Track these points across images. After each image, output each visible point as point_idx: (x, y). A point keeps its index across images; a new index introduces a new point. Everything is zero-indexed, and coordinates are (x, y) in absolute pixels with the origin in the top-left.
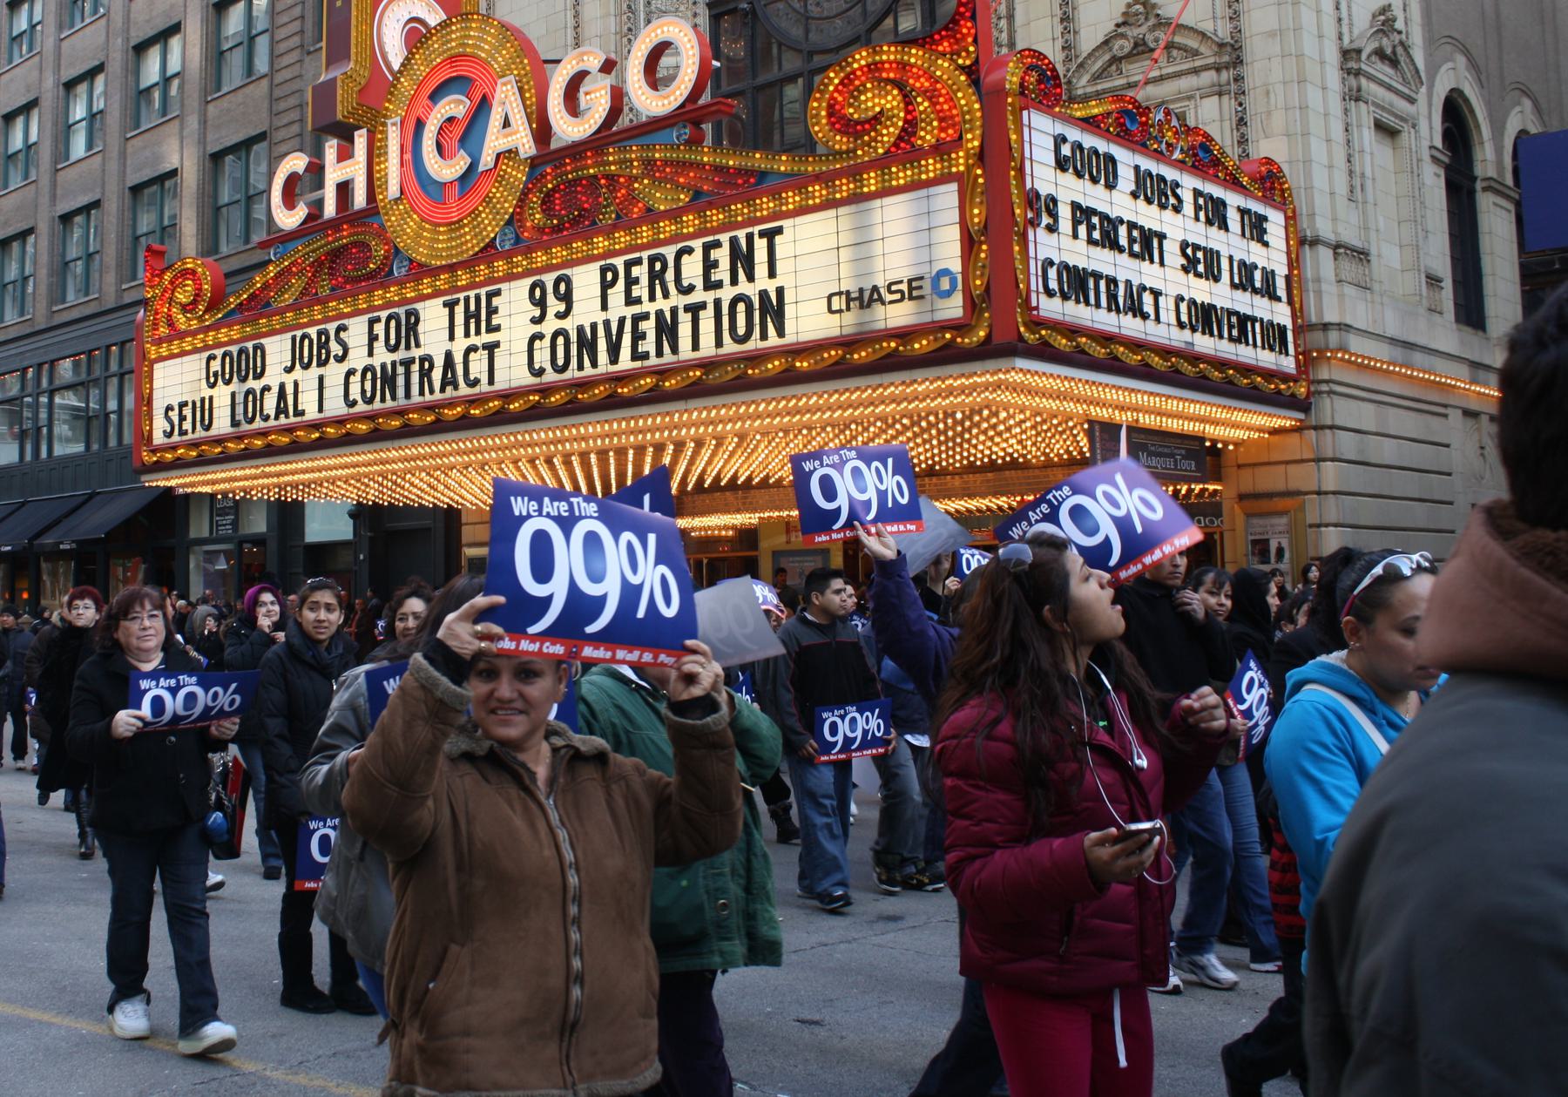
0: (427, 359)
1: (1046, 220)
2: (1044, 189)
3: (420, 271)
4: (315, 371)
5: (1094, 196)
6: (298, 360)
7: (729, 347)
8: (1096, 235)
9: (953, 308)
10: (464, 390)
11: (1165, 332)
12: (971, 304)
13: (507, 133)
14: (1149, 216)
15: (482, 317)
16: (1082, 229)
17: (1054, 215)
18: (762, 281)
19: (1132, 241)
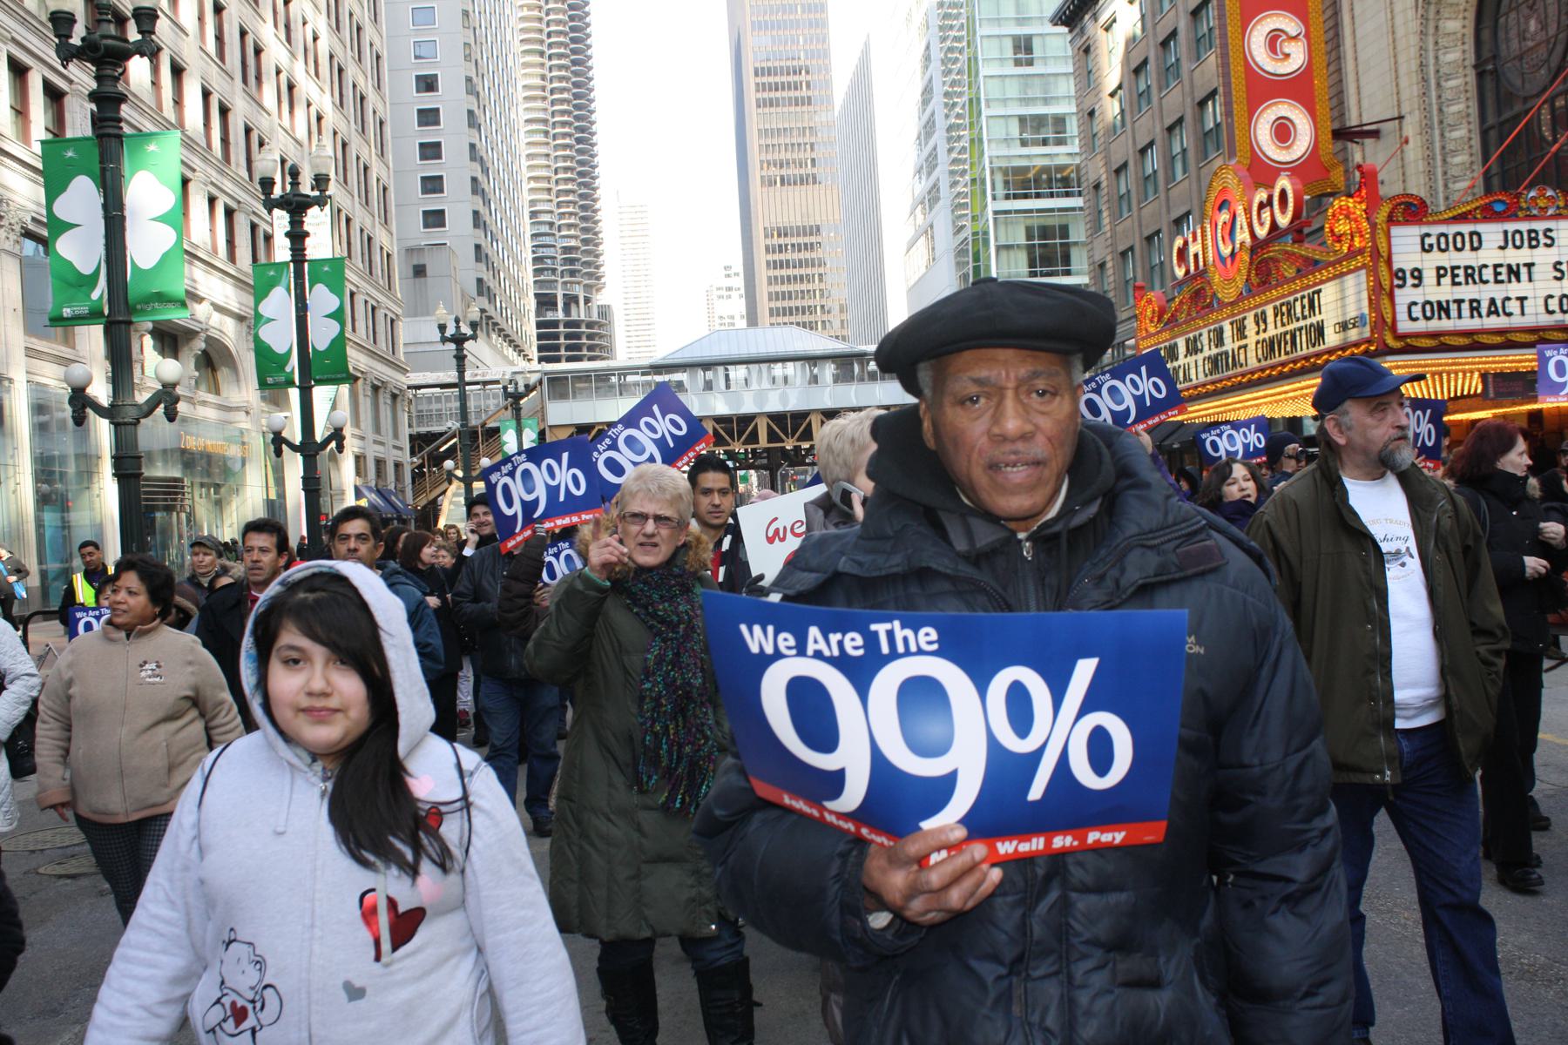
0: (1226, 353)
1: (1410, 281)
2: (1408, 267)
3: (1222, 305)
4: (1194, 357)
5: (1466, 258)
6: (1189, 352)
7: (1312, 350)
8: (1461, 279)
9: (1367, 334)
10: (1239, 370)
11: (1534, 315)
12: (1372, 332)
13: (1243, 236)
14: (1514, 257)
15: (1241, 332)
16: (1447, 280)
17: (1420, 278)
18: (1319, 318)
19: (1497, 274)
